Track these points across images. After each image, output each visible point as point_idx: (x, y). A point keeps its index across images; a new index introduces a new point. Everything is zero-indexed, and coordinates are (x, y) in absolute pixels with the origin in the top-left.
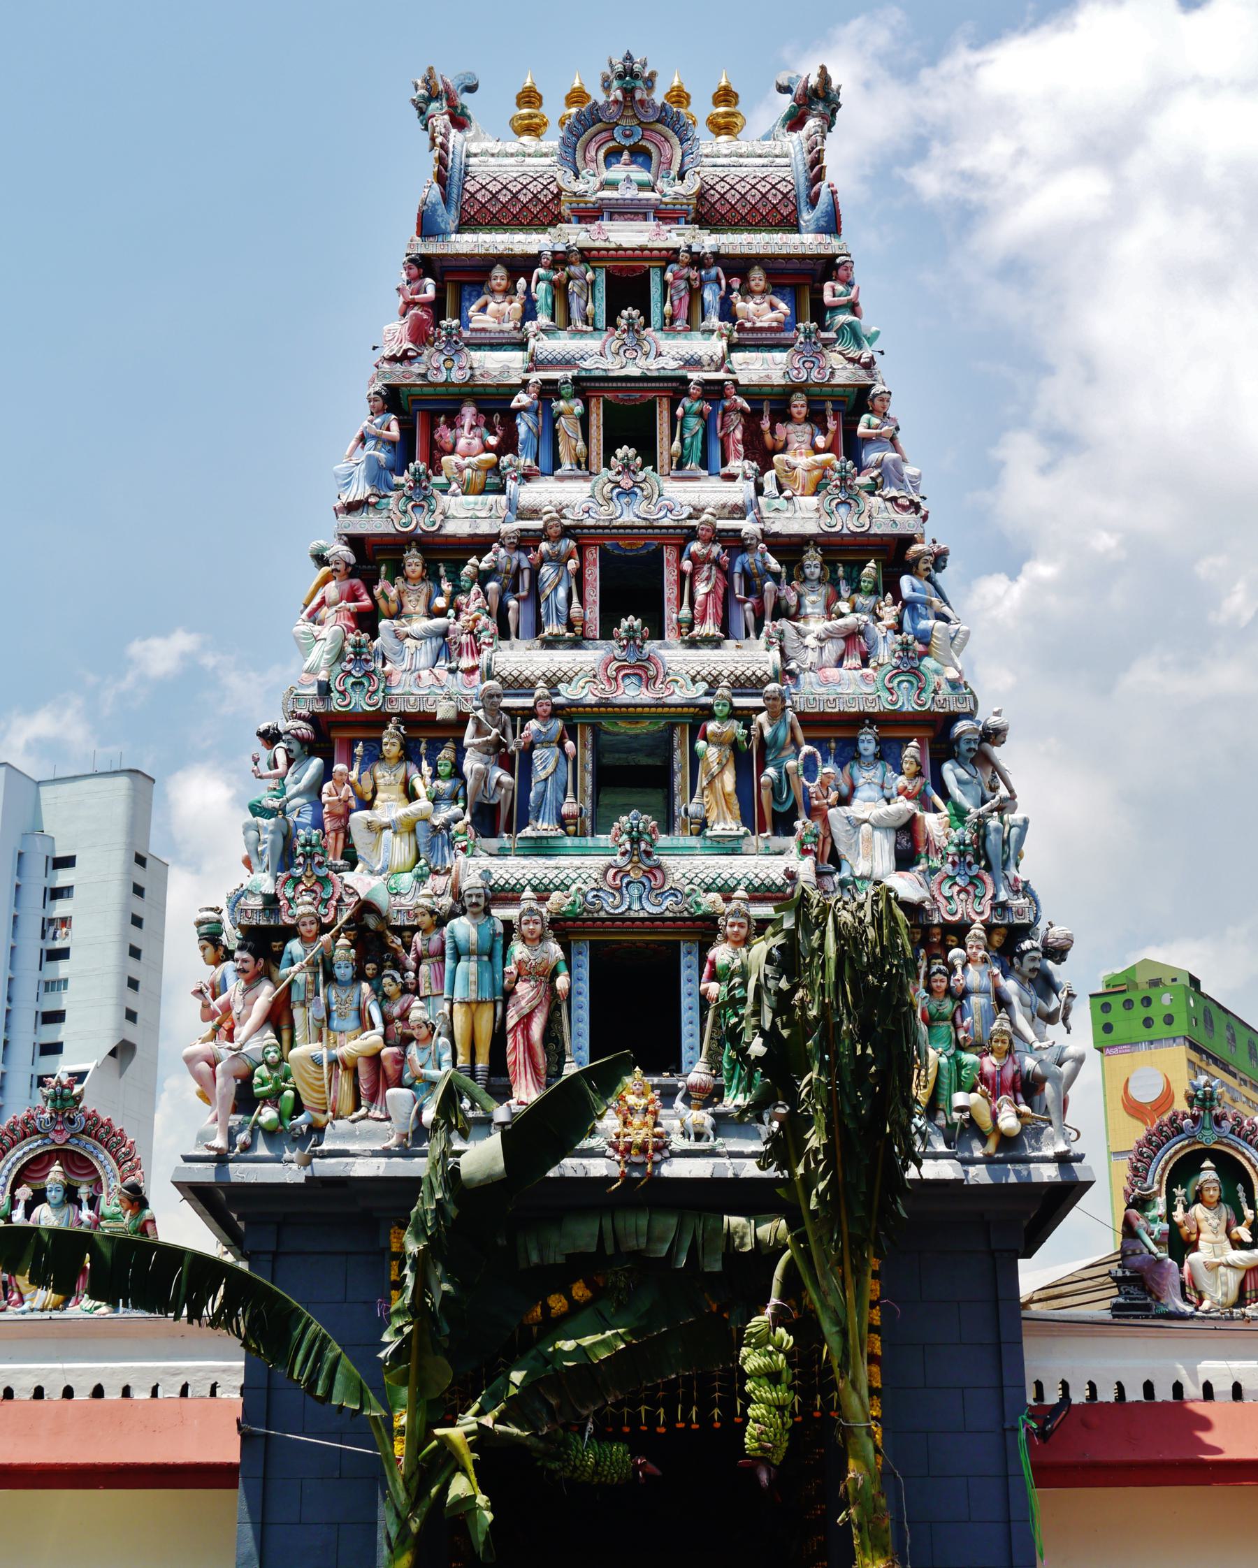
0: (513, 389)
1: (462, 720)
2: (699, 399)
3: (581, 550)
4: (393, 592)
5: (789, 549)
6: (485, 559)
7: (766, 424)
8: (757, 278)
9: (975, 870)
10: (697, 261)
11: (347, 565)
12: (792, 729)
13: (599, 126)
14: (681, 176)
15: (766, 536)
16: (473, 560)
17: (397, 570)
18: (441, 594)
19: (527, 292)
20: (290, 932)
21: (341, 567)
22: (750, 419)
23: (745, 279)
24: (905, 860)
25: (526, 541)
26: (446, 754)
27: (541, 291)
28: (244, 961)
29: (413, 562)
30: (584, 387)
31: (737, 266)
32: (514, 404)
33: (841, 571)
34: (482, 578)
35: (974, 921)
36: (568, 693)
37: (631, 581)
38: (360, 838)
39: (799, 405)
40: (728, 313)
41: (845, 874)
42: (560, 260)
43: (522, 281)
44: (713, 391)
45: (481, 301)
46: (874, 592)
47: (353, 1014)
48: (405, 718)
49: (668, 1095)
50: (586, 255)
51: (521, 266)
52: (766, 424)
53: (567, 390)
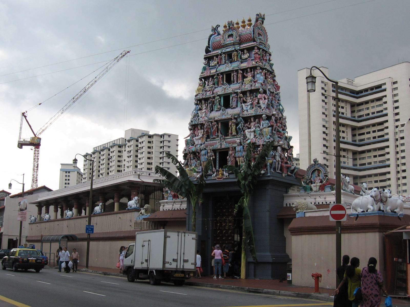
2: (235, 72)
3: (220, 98)
5: (244, 93)
8: (245, 51)
9: (262, 137)
10: (237, 51)
14: (237, 37)
23: (244, 52)
25: (214, 97)
30: (222, 73)
31: (242, 50)
36: (216, 119)
38: (195, 140)
39: (249, 70)
40: (241, 58)
42: (221, 55)
44: (237, 71)
48: (200, 124)
49: (223, 171)
50: (224, 53)
51: (217, 56)
53: (220, 74)
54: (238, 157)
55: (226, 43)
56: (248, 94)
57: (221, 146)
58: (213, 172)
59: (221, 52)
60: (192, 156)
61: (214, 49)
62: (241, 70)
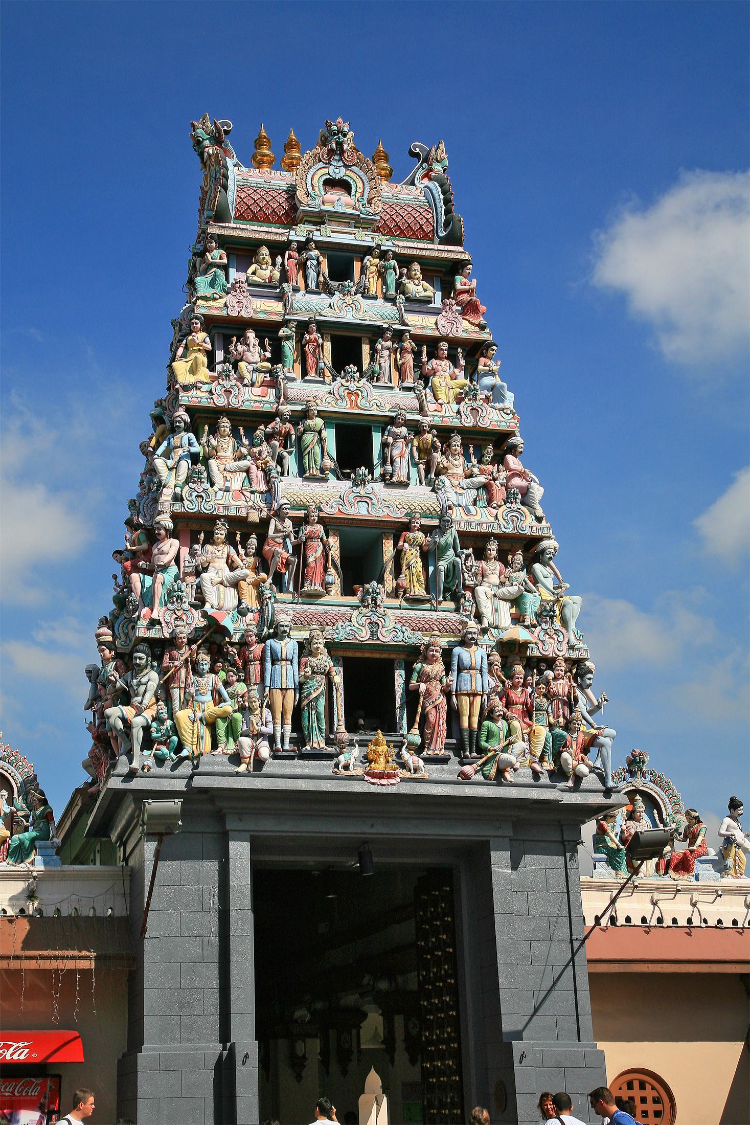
0: (279, 325)
1: (265, 522)
4: (214, 442)
6: (270, 426)
7: (424, 358)
10: (383, 255)
11: (185, 423)
12: (455, 539)
13: (321, 165)
15: (432, 427)
16: (262, 427)
17: (214, 430)
18: (241, 444)
19: (283, 264)
20: (171, 643)
21: (182, 425)
22: (417, 355)
24: (517, 619)
26: (253, 541)
27: (291, 265)
28: (141, 658)
29: (225, 424)
30: (324, 327)
31: (405, 261)
32: (281, 333)
33: (471, 450)
34: (269, 437)
35: (558, 656)
37: (355, 445)
41: (485, 624)
42: (303, 247)
43: (279, 259)
44: (398, 336)
45: (253, 267)
46: (492, 463)
47: (210, 693)
49: (399, 745)
50: (320, 246)
51: (278, 249)
52: (424, 358)
54: (468, 695)
55: (323, 208)
56: (457, 440)
57: (374, 634)
58: (329, 742)
59: (309, 240)
60: (205, 659)
61: (240, 217)
62: (414, 338)
